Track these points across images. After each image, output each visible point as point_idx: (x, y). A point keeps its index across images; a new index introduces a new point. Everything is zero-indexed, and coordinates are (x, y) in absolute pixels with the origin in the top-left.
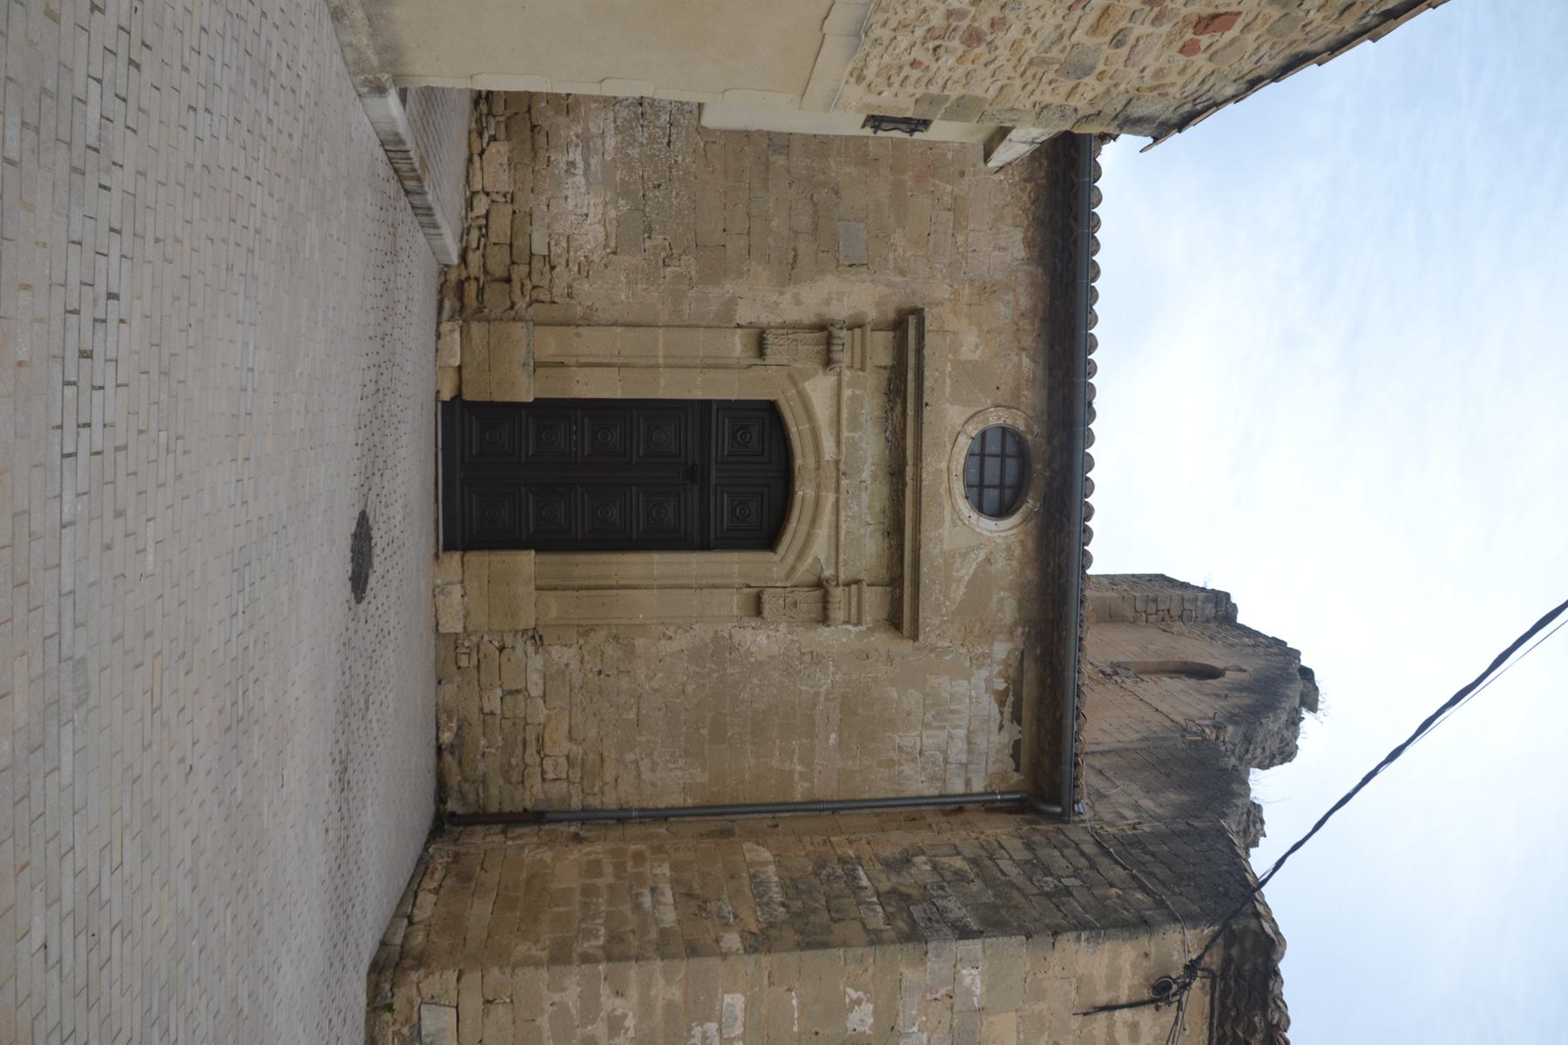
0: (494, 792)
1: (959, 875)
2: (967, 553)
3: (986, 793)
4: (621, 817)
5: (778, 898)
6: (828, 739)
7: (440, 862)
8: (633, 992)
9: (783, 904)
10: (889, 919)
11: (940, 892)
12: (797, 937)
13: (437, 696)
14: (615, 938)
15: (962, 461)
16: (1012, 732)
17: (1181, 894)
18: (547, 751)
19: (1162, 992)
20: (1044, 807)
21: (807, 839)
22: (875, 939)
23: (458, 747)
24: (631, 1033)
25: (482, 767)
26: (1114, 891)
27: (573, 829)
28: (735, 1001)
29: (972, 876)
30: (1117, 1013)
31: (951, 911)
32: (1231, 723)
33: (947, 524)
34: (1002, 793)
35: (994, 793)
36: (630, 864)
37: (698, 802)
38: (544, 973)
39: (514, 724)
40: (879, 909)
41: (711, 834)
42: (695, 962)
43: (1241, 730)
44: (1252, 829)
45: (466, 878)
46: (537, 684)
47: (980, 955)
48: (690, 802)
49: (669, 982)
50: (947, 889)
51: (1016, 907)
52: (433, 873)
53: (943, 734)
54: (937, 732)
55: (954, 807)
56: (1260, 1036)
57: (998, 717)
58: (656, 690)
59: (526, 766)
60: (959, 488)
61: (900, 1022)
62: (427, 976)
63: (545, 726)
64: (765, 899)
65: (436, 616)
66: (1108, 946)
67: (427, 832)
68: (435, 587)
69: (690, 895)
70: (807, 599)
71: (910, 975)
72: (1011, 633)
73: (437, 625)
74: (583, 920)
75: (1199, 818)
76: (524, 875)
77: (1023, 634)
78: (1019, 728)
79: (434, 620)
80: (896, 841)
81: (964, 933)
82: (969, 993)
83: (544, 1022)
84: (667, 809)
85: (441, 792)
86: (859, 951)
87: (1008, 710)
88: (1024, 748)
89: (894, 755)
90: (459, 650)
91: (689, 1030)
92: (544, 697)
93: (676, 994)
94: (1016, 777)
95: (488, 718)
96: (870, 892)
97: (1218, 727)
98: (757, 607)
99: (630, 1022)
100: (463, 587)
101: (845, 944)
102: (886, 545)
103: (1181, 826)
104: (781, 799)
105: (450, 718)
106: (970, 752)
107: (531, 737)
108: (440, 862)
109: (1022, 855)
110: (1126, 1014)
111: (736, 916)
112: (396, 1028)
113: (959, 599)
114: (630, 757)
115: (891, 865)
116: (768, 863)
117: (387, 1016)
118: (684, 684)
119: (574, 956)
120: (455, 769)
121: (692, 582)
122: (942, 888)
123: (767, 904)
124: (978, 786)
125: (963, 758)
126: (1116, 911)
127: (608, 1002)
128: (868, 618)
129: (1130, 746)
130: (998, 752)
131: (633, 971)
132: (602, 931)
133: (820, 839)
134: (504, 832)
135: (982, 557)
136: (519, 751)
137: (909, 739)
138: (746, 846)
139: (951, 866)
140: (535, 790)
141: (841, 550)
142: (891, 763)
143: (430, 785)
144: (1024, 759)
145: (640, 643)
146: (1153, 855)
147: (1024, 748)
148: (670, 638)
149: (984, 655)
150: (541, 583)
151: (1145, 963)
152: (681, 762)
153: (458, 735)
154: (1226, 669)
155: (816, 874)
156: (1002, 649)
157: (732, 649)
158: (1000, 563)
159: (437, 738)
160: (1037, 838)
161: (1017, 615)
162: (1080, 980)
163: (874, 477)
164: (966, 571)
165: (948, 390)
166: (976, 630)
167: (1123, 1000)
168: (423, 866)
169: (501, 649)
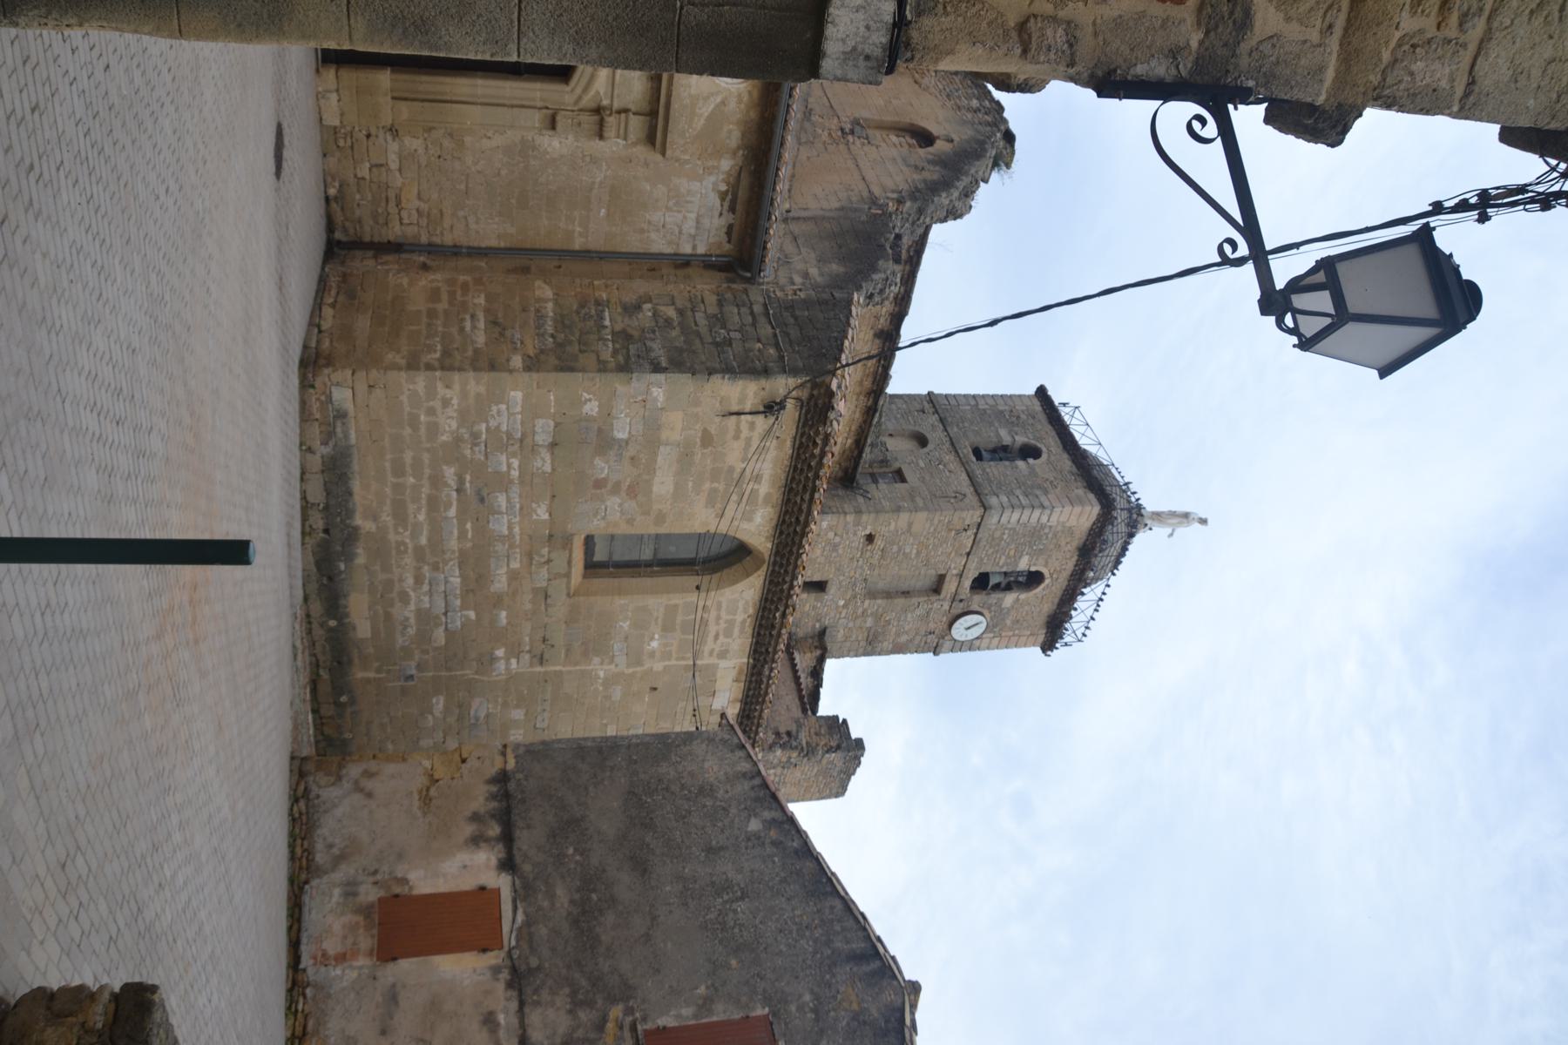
0: (367, 229)
1: (668, 321)
2: (708, 97)
3: (706, 255)
4: (455, 251)
5: (550, 330)
6: (599, 212)
7: (333, 281)
8: (457, 387)
9: (552, 336)
10: (615, 352)
11: (652, 335)
12: (557, 362)
13: (323, 164)
14: (446, 353)
16: (728, 218)
17: (798, 352)
18: (403, 205)
19: (771, 408)
20: (741, 273)
21: (578, 281)
22: (602, 368)
23: (341, 197)
24: (456, 407)
25: (358, 213)
26: (759, 345)
27: (422, 259)
28: (517, 395)
29: (675, 324)
30: (743, 417)
31: (654, 351)
32: (911, 199)
34: (717, 256)
35: (711, 256)
36: (459, 292)
37: (508, 245)
38: (403, 374)
39: (379, 187)
40: (610, 344)
41: (515, 270)
42: (493, 374)
43: (916, 206)
44: (887, 290)
45: (352, 296)
46: (394, 161)
47: (663, 381)
48: (502, 245)
49: (478, 383)
50: (657, 333)
51: (694, 352)
52: (330, 290)
53: (680, 216)
54: (676, 214)
55: (682, 263)
56: (821, 437)
57: (720, 208)
58: (479, 172)
59: (388, 214)
61: (614, 411)
62: (334, 371)
63: (401, 189)
64: (542, 331)
65: (320, 113)
66: (741, 382)
67: (322, 254)
68: (318, 94)
69: (495, 323)
70: (589, 120)
71: (621, 389)
72: (734, 153)
73: (321, 119)
74: (427, 337)
75: (842, 288)
76: (389, 298)
77: (743, 155)
78: (732, 216)
79: (318, 115)
80: (640, 287)
81: (657, 368)
82: (655, 400)
83: (404, 398)
84: (486, 248)
85: (330, 226)
86: (591, 375)
87: (726, 204)
88: (736, 229)
89: (645, 226)
90: (338, 135)
91: (490, 407)
92: (400, 170)
93: (482, 389)
94: (727, 247)
95: (362, 182)
96: (608, 331)
97: (900, 202)
98: (552, 124)
99: (455, 401)
100: (339, 95)
101: (583, 370)
102: (649, 86)
103: (825, 296)
104: (565, 248)
105: (334, 179)
106: (697, 228)
107: (392, 194)
108: (333, 281)
109: (713, 309)
110: (749, 417)
111: (522, 343)
112: (317, 396)
113: (699, 128)
114: (461, 213)
115: (632, 309)
116: (549, 300)
117: (311, 391)
118: (499, 170)
119: (422, 365)
120: (339, 213)
121: (506, 102)
122: (654, 332)
123: (543, 335)
124: (701, 250)
125: (693, 231)
126: (753, 361)
127: (441, 391)
128: (632, 137)
129: (827, 214)
130: (717, 230)
131: (456, 377)
132: (439, 347)
133: (587, 281)
134: (375, 257)
135: (719, 100)
136: (383, 204)
137: (657, 217)
138: (538, 283)
139: (665, 314)
140: (395, 230)
141: (616, 87)
142: (642, 231)
143: (323, 222)
144: (735, 236)
145: (468, 139)
146: (796, 318)
147: (736, 229)
148: (489, 138)
149: (714, 167)
150: (396, 94)
151: (762, 393)
152: (497, 219)
153: (340, 190)
154: (938, 138)
156: (726, 164)
157: (534, 148)
158: (732, 105)
159: (326, 192)
160: (729, 296)
161: (740, 142)
162: (722, 398)
164: (706, 110)
166: (709, 150)
167: (747, 410)
168: (322, 284)
169: (368, 136)
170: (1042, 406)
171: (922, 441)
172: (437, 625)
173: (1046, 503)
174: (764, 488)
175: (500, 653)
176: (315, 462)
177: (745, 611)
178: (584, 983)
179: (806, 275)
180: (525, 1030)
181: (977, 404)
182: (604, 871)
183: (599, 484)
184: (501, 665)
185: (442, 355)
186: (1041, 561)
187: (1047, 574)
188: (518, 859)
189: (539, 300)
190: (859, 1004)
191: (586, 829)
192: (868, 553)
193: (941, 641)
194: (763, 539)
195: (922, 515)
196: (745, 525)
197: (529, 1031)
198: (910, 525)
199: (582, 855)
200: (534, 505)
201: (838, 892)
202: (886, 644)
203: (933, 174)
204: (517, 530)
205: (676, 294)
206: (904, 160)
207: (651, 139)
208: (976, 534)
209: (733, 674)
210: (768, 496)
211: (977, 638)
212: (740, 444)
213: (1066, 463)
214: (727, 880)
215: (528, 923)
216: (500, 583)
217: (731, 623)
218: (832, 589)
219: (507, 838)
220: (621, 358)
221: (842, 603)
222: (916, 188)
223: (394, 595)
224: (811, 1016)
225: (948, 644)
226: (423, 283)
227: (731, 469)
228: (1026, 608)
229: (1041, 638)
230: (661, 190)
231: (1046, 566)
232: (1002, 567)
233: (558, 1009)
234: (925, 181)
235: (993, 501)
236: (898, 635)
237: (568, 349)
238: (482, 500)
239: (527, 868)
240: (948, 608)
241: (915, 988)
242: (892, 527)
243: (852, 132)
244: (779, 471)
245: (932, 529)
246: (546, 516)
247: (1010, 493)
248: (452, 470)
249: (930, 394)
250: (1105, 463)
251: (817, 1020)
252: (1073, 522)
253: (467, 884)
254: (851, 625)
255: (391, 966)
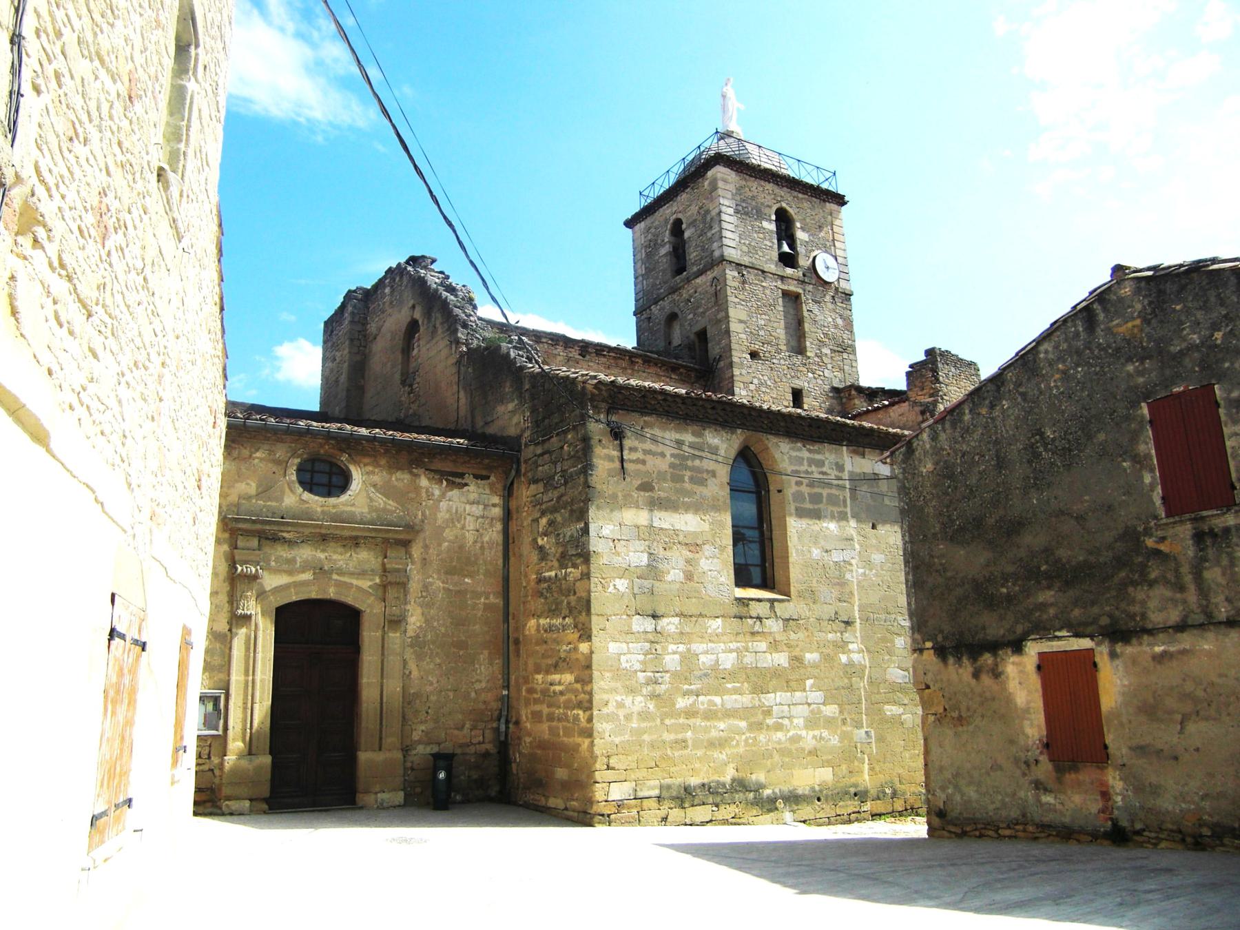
1: (551, 523)
5: (560, 620)
6: (468, 583)
8: (605, 697)
9: (564, 618)
10: (575, 566)
11: (561, 536)
12: (584, 614)
14: (579, 705)
15: (317, 498)
19: (617, 435)
22: (587, 576)
24: (624, 697)
26: (565, 447)
28: (613, 647)
33: (353, 509)
36: (536, 696)
40: (569, 570)
47: (596, 525)
54: (467, 521)
55: (507, 516)
60: (332, 500)
65: (395, 807)
69: (556, 666)
71: (604, 560)
74: (568, 721)
81: (586, 531)
83: (617, 740)
86: (592, 585)
99: (619, 698)
101: (589, 592)
103: (527, 395)
106: (478, 503)
109: (540, 487)
110: (626, 453)
111: (570, 643)
113: (395, 505)
114: (473, 694)
118: (436, 665)
119: (588, 726)
122: (558, 535)
124: (496, 500)
125: (481, 507)
126: (577, 451)
130: (479, 487)
131: (597, 698)
137: (470, 537)
142: (482, 548)
152: (477, 666)
154: (412, 317)
155: (546, 598)
156: (424, 482)
157: (417, 636)
158: (376, 478)
163: (323, 551)
165: (274, 504)
167: (619, 454)
170: (640, 222)
171: (672, 317)
172: (820, 712)
173: (717, 210)
174: (688, 438)
175: (844, 658)
176: (676, 814)
177: (800, 450)
178: (1123, 574)
179: (513, 412)
180: (1169, 627)
181: (642, 275)
182: (1021, 559)
183: (689, 577)
184: (856, 657)
185: (581, 708)
186: (767, 211)
187: (777, 206)
188: (1011, 637)
189: (538, 630)
190: (1133, 319)
191: (985, 577)
192: (767, 355)
193: (840, 290)
194: (734, 436)
195: (732, 312)
196: (722, 452)
197: (1170, 623)
198: (741, 321)
199: (1007, 581)
200: (709, 631)
201: (1032, 348)
202: (845, 336)
203: (438, 317)
204: (733, 645)
205: (530, 519)
206: (428, 343)
207: (406, 544)
208: (746, 267)
209: (858, 459)
210: (694, 434)
211: (836, 259)
212: (648, 458)
213: (683, 197)
214: (1025, 449)
215: (1068, 625)
216: (781, 659)
217: (811, 462)
218: (798, 384)
219: (994, 647)
220: (579, 561)
221: (810, 375)
222: (447, 330)
223: (793, 748)
224: (1147, 364)
225: (843, 284)
226: (528, 725)
227: (672, 466)
228: (808, 220)
229: (833, 206)
230: (448, 534)
231: (770, 207)
232: (773, 243)
233: (1148, 597)
234: (442, 323)
235: (717, 254)
236: (836, 327)
237: (573, 604)
238: (706, 675)
239: (1019, 629)
240: (812, 286)
241: (1118, 270)
242: (743, 336)
243: (411, 386)
244: (672, 425)
245: (743, 303)
246: (719, 621)
247: (711, 240)
248: (680, 700)
249: (635, 314)
250: (682, 167)
251: (1150, 357)
252: (732, 187)
253: (1035, 681)
254: (829, 366)
255: (1112, 749)
